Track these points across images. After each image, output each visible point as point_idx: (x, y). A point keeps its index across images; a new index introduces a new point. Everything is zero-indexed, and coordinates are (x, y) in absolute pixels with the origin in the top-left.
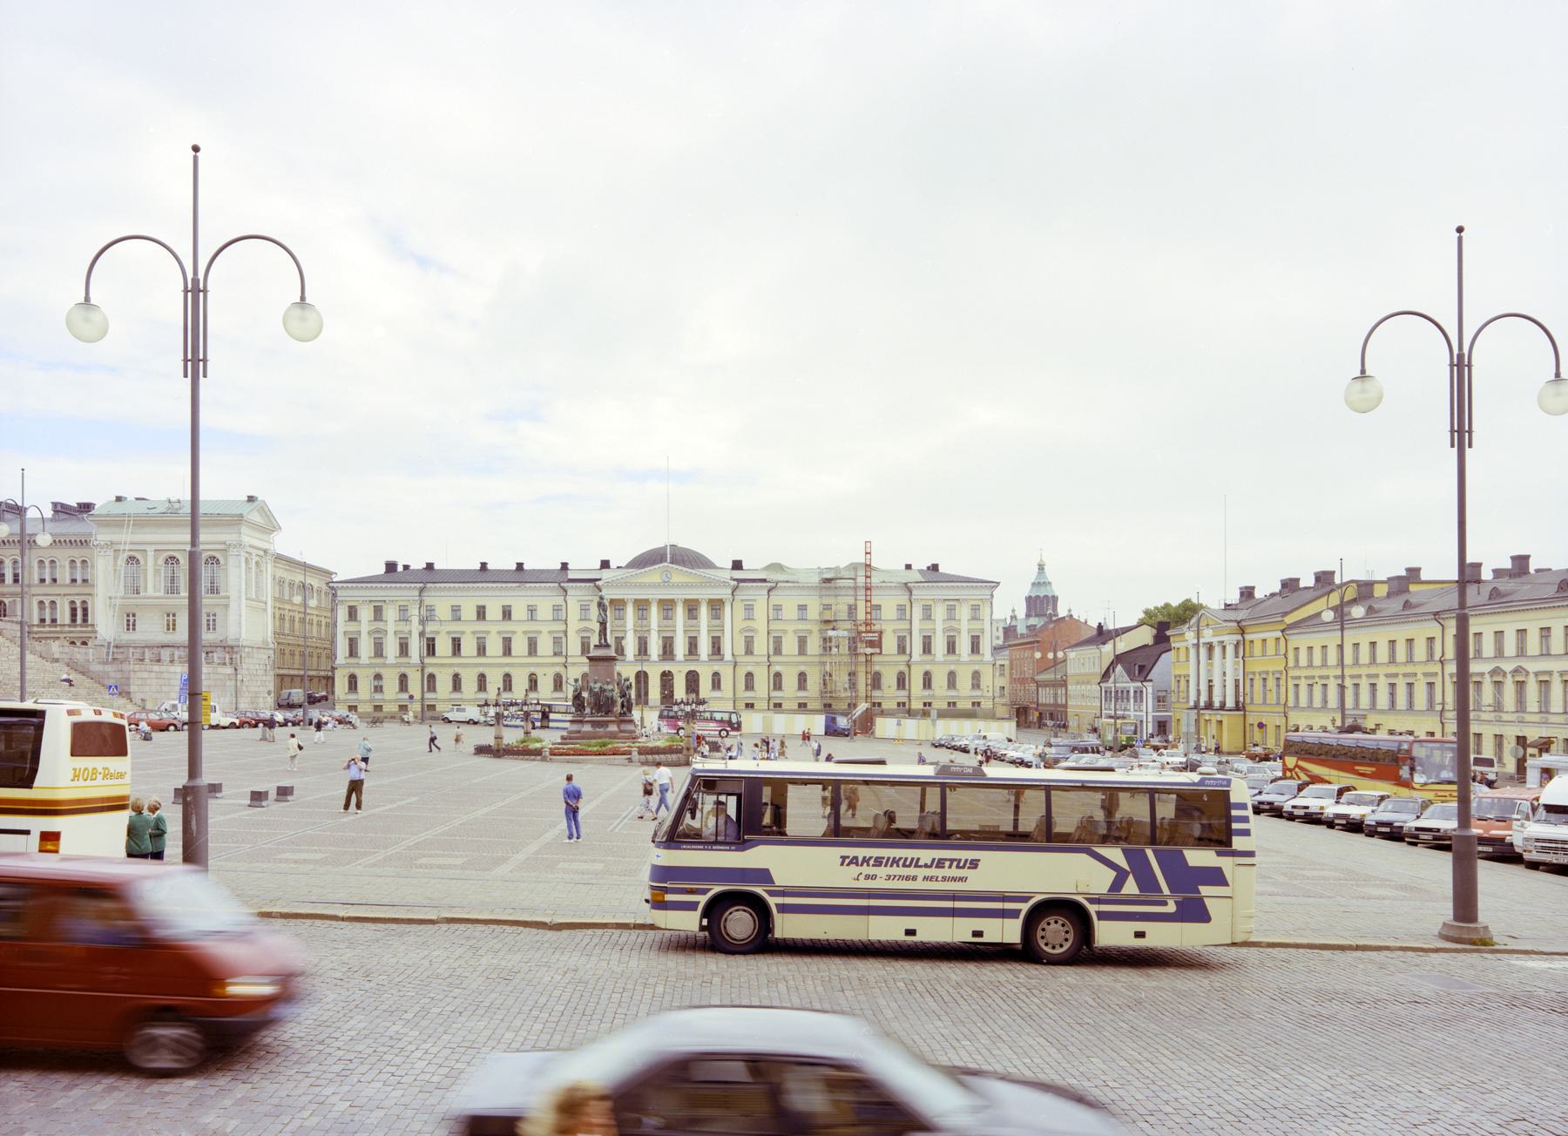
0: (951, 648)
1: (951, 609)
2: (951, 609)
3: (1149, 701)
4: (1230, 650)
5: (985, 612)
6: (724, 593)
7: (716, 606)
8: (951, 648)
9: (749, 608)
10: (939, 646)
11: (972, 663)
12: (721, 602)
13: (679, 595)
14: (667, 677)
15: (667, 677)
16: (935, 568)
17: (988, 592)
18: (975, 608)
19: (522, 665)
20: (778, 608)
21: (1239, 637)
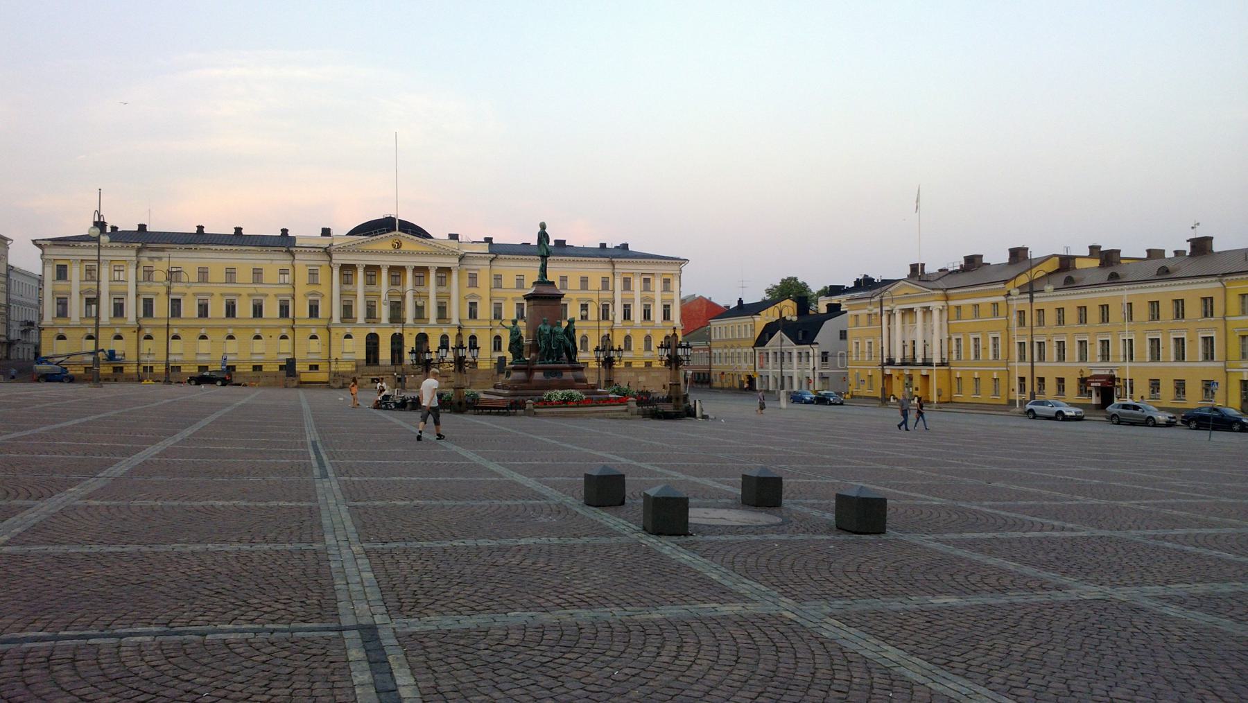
0: (647, 315)
1: (647, 281)
2: (647, 281)
3: (815, 361)
4: (936, 314)
5: (674, 284)
6: (452, 262)
7: (444, 271)
8: (647, 315)
9: (473, 278)
10: (637, 314)
11: (643, 328)
12: (449, 270)
13: (410, 262)
14: (397, 340)
15: (397, 340)
16: (625, 246)
17: (676, 267)
18: (667, 281)
19: (247, 328)
20: (498, 278)
21: (943, 303)
